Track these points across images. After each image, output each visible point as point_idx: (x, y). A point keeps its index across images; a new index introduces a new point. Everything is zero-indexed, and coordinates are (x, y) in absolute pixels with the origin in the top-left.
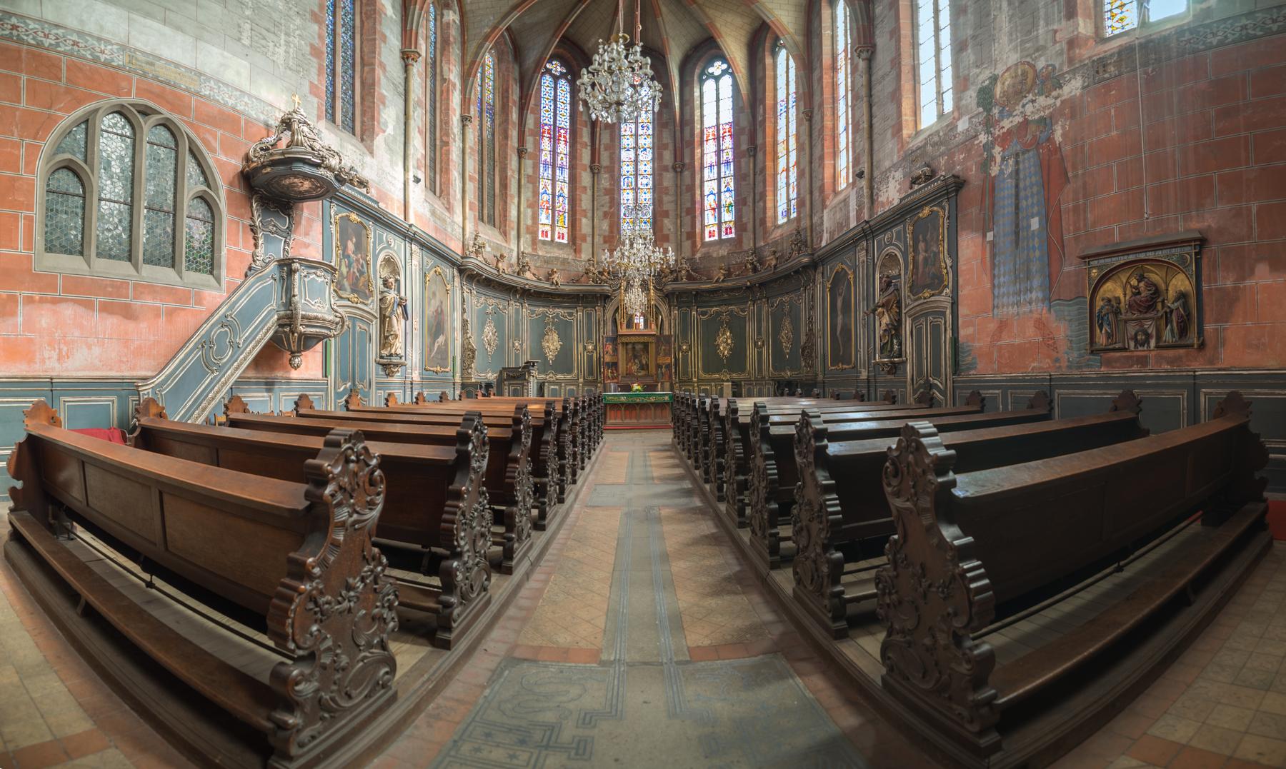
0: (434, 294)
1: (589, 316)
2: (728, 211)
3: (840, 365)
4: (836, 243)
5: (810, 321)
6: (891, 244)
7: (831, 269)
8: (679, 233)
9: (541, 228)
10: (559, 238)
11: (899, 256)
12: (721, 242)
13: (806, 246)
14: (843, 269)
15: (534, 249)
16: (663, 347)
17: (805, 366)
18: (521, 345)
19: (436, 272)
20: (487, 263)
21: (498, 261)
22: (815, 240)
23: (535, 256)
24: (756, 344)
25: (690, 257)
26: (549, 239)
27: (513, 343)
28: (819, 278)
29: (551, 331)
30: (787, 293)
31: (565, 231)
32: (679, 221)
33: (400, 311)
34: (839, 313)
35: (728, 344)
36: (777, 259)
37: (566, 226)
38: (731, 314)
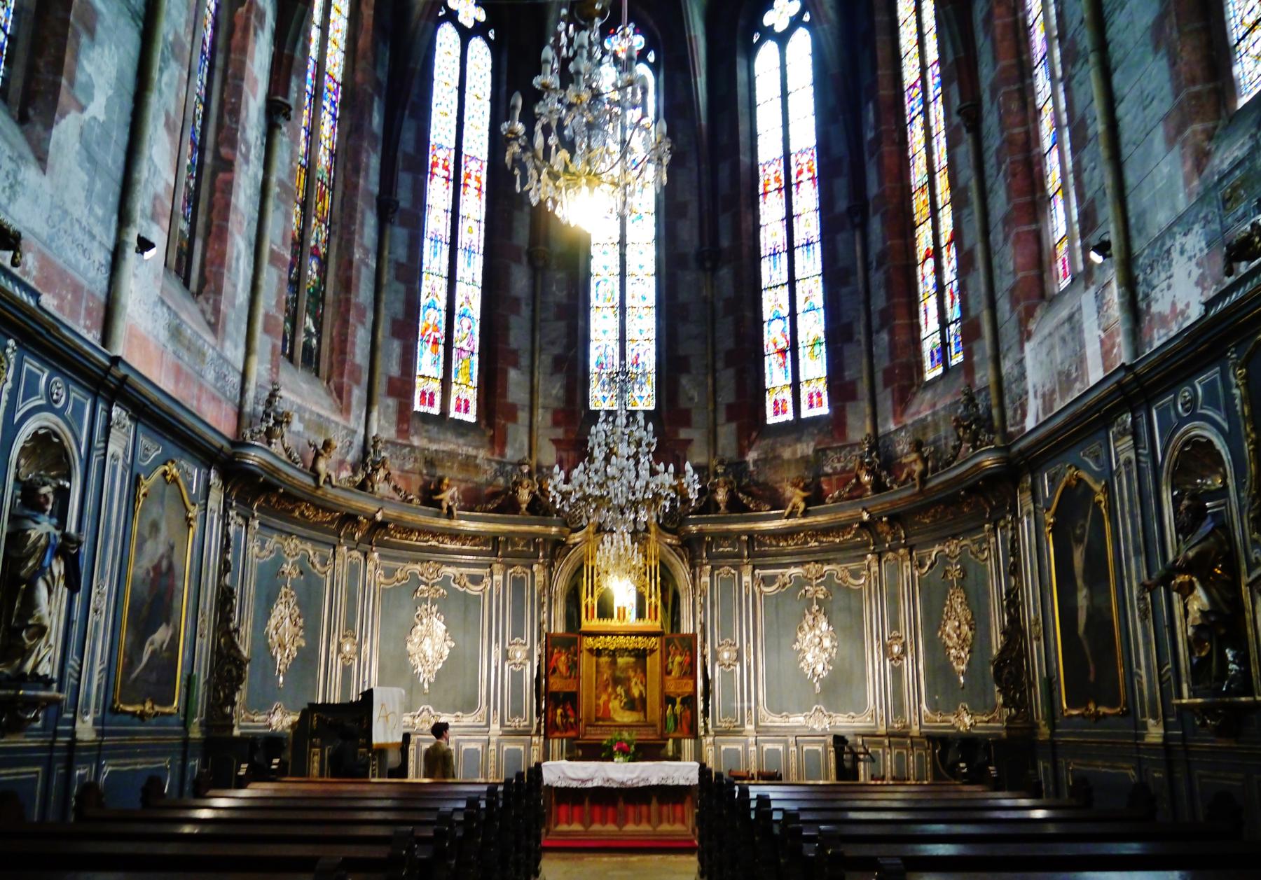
0: (155, 527)
1: (518, 583)
2: (813, 355)
3: (1092, 707)
4: (1059, 421)
5: (1013, 602)
6: (1194, 416)
7: (1051, 480)
8: (711, 407)
9: (420, 385)
10: (458, 409)
11: (1219, 444)
12: (798, 426)
13: (991, 430)
14: (1080, 480)
15: (402, 433)
16: (678, 659)
17: (1005, 705)
18: (360, 646)
19: (165, 474)
20: (293, 462)
21: (318, 455)
22: (1009, 413)
23: (406, 446)
24: (887, 650)
25: (736, 459)
26: (436, 410)
27: (340, 646)
28: (1025, 502)
29: (429, 615)
30: (955, 536)
31: (471, 395)
32: (710, 381)
33: (58, 568)
34: (1080, 582)
36: (925, 461)
37: (475, 383)
38: (829, 581)
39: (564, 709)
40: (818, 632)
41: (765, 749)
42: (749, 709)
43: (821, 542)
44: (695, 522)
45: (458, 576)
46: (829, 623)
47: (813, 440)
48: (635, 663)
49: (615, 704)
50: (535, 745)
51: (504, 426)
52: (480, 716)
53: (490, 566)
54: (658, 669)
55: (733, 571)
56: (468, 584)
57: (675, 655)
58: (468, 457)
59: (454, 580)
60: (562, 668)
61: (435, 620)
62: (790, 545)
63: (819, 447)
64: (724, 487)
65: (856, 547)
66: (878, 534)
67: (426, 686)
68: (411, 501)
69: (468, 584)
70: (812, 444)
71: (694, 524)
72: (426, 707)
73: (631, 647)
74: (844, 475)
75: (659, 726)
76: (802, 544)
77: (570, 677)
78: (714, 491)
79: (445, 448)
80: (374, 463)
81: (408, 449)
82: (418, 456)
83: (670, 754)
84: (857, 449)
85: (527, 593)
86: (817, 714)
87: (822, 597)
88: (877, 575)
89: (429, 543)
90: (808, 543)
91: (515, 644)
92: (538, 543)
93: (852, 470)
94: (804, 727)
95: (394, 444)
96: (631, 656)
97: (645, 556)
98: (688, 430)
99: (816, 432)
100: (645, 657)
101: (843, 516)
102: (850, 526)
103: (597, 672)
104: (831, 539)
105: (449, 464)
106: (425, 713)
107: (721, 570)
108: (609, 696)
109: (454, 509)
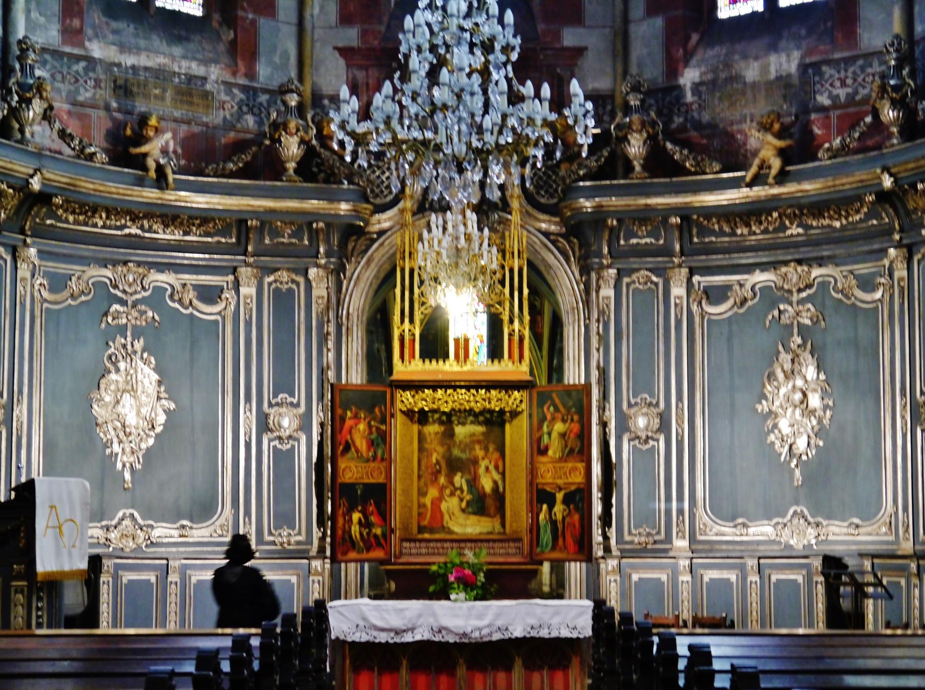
16: (559, 427)
23: (78, 58)
29: (129, 356)
35: (809, 412)
39: (364, 513)
40: (799, 383)
41: (706, 579)
42: (680, 512)
43: (807, 227)
44: (590, 193)
45: (178, 287)
46: (819, 368)
47: (798, 48)
48: (483, 434)
49: (451, 504)
50: (317, 573)
51: (253, 23)
52: (222, 526)
53: (234, 270)
54: (524, 444)
55: (655, 279)
56: (196, 302)
57: (554, 419)
58: (190, 78)
59: (171, 297)
60: (361, 443)
61: (140, 364)
62: (754, 234)
63: (808, 61)
64: (640, 132)
65: (870, 235)
66: (908, 213)
67: (127, 476)
68: (91, 157)
69: (196, 302)
70: (796, 55)
71: (587, 198)
72: (129, 511)
73: (478, 407)
74: (851, 110)
75: (526, 540)
76: (776, 230)
77: (375, 458)
78: (625, 139)
79: (149, 64)
80: (23, 87)
81: (83, 64)
82: (102, 77)
83: (546, 589)
84: (876, 63)
85: (300, 316)
86: (795, 521)
87: (808, 322)
88: (905, 284)
89: (127, 231)
90: (784, 228)
91: (277, 404)
92: (317, 230)
93: (866, 100)
94: (773, 542)
95: (57, 54)
96: (480, 423)
97: (502, 252)
98: (581, 30)
99: (803, 32)
100: (502, 425)
101: (846, 182)
102: (860, 199)
103: (421, 449)
104: (826, 222)
105: (157, 92)
106: (127, 522)
107: (634, 277)
108: (442, 489)
109: (169, 171)
